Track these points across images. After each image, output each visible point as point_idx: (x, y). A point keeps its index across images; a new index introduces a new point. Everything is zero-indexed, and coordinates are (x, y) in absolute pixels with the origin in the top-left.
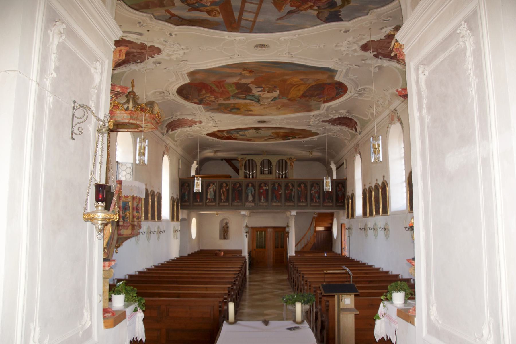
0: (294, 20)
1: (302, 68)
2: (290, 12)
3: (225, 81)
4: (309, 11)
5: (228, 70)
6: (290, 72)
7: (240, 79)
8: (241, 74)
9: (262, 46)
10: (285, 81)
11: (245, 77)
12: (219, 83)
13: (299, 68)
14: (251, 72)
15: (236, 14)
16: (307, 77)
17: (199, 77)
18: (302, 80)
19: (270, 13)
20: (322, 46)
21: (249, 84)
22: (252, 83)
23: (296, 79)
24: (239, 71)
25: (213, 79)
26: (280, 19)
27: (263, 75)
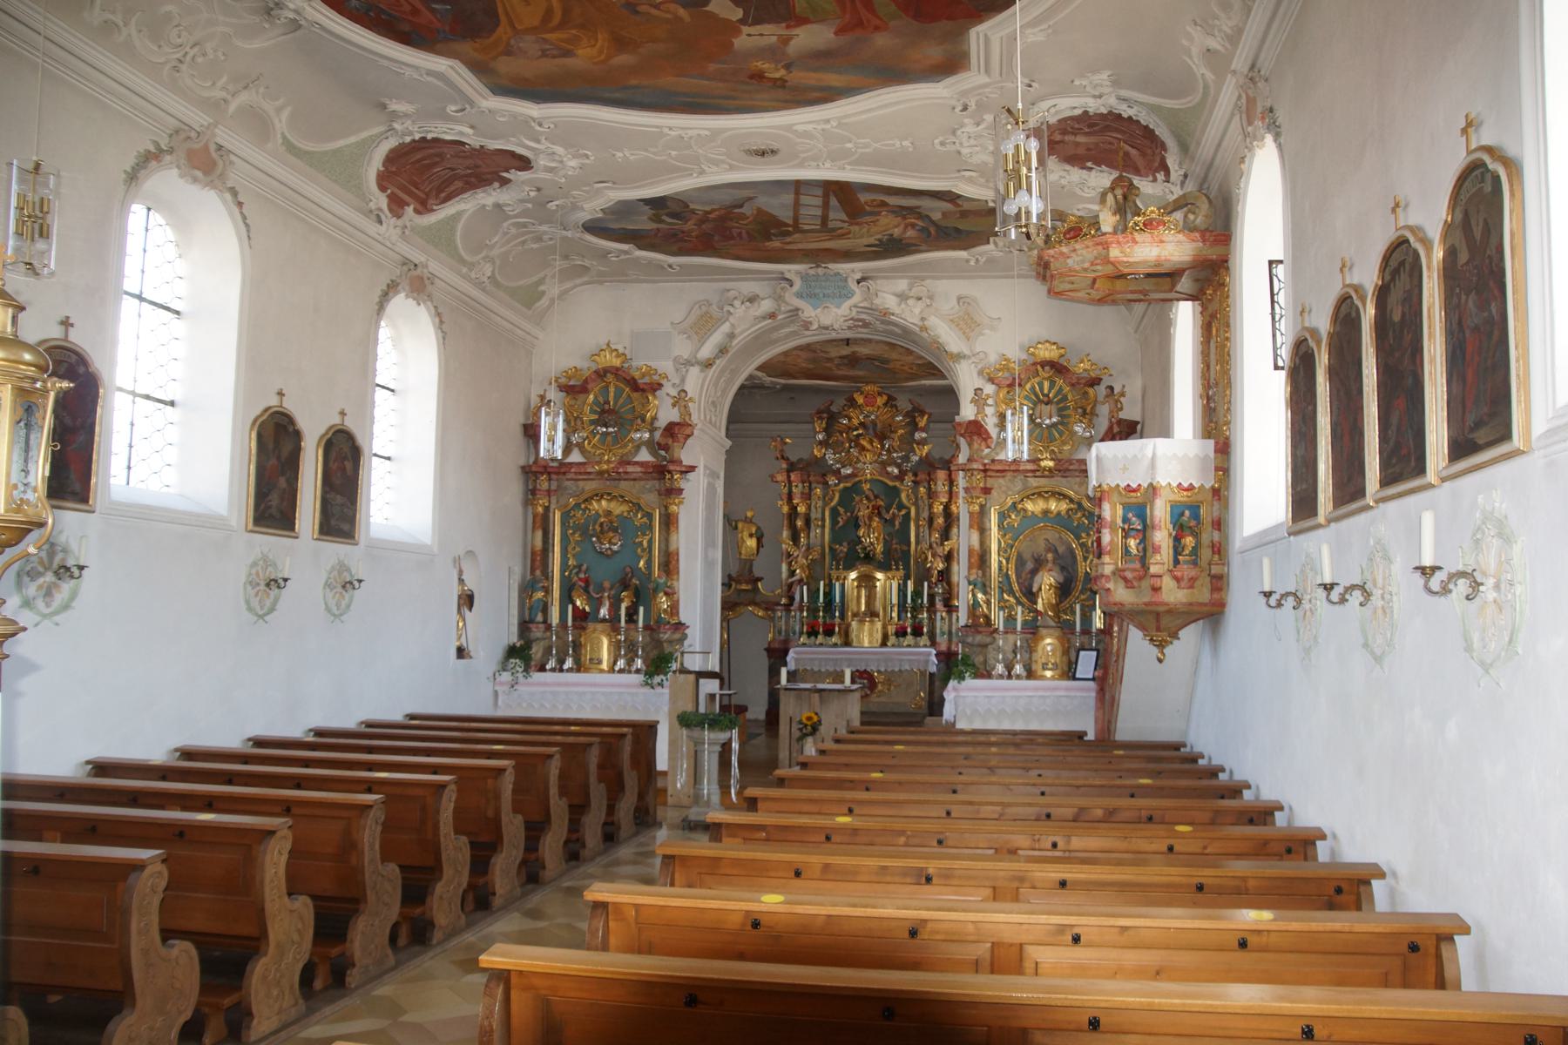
0: (727, 198)
1: (607, 95)
2: (741, 206)
3: (836, 33)
4: (708, 208)
5: (833, 80)
6: (634, 82)
7: (786, 41)
8: (788, 67)
9: (763, 153)
10: (620, 43)
11: (774, 53)
12: (860, 24)
13: (618, 95)
14: (759, 76)
15: (833, 201)
16: (557, 61)
17: (934, 52)
18: (568, 54)
19: (780, 207)
20: (619, 154)
21: (743, 21)
22: (732, 29)
23: (585, 56)
24: (798, 77)
25: (882, 41)
26: (750, 199)
27: (712, 67)
